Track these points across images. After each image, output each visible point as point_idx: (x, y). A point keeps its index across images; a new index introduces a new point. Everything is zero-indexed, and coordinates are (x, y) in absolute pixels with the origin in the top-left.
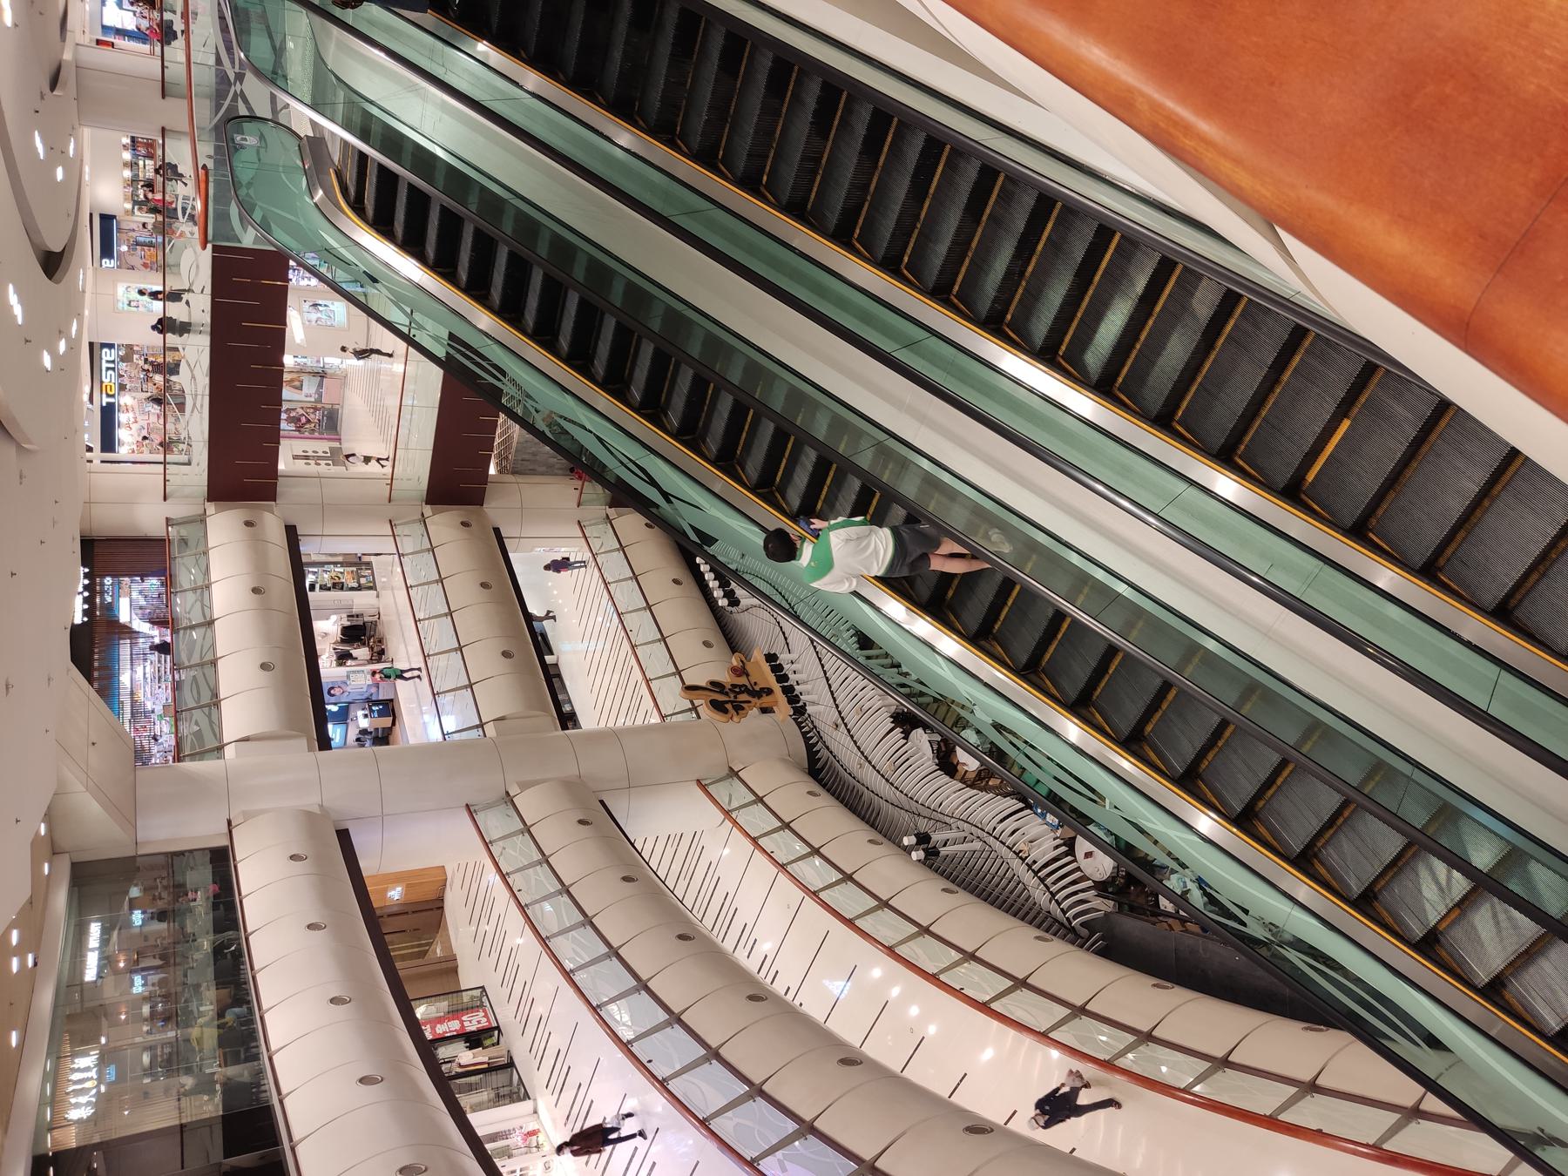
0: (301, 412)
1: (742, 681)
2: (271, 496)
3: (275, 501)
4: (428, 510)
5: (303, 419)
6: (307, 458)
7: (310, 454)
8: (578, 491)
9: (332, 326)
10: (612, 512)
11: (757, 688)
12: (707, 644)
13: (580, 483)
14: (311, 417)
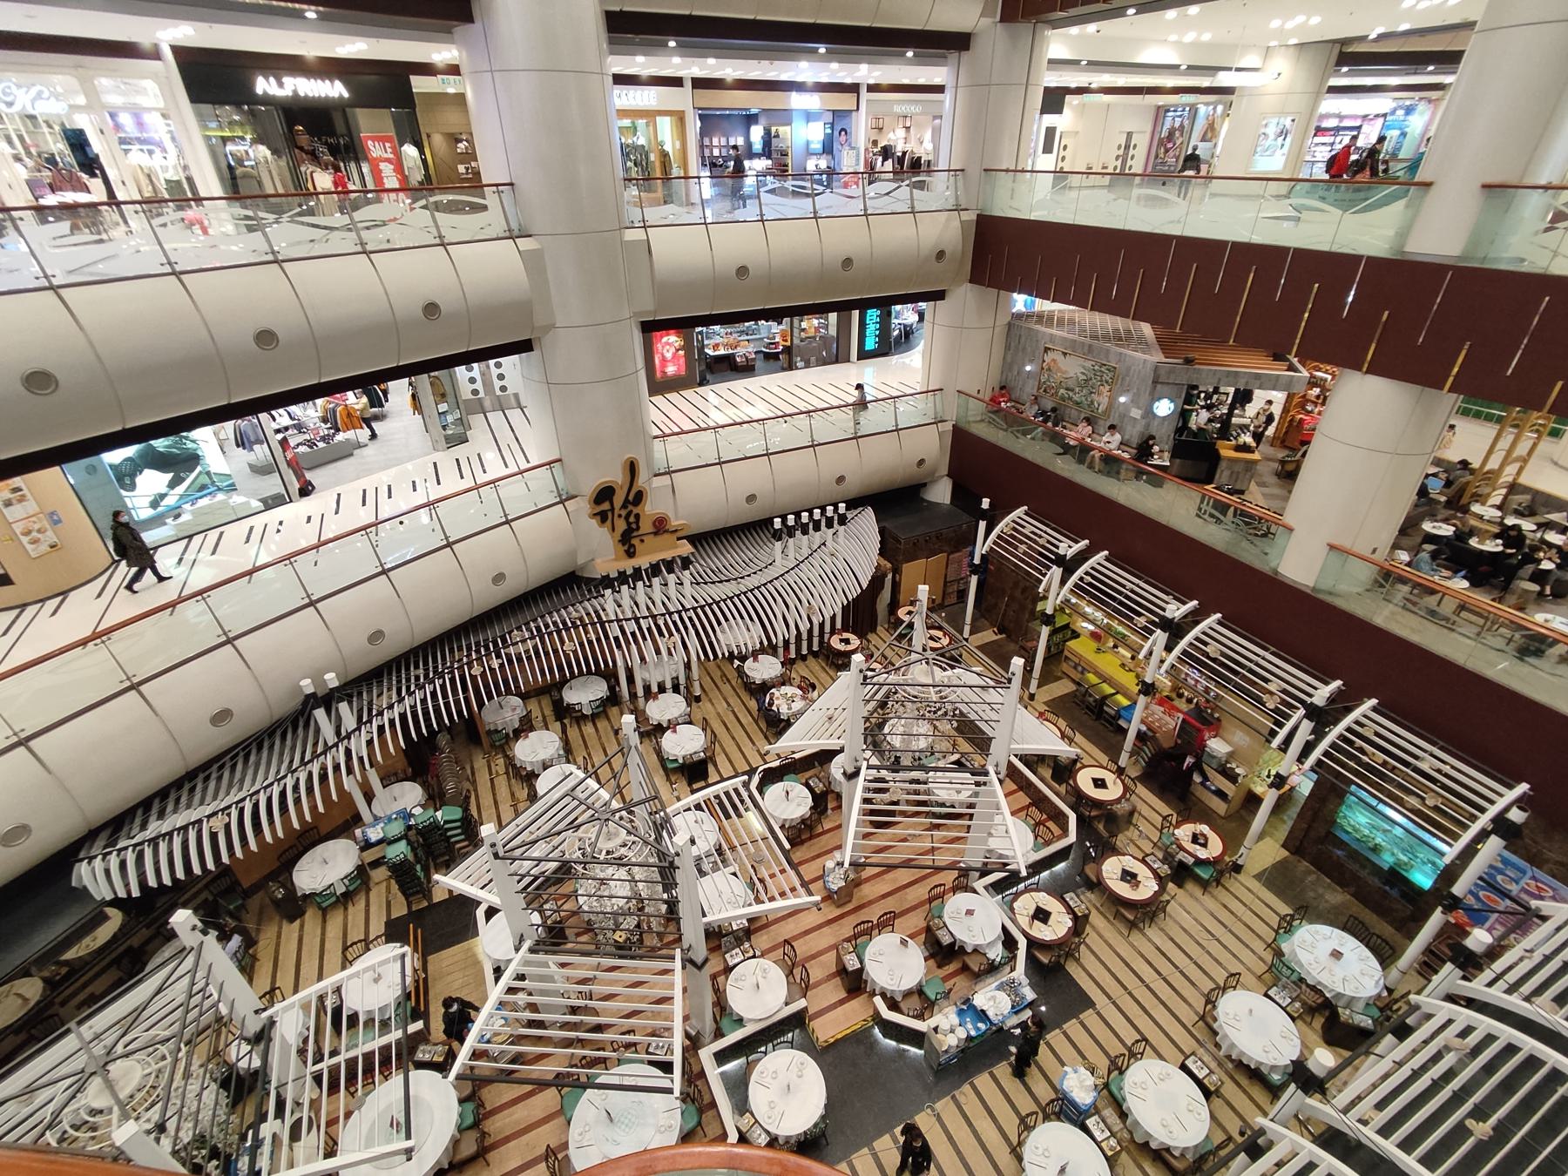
0: (1178, 142)
1: (646, 526)
2: (1006, 17)
3: (1001, 21)
4: (970, 216)
5: (1170, 145)
6: (1127, 147)
7: (1131, 152)
8: (975, 394)
9: (1255, 152)
10: (948, 427)
11: (635, 542)
12: (751, 498)
13: (987, 398)
14: (1171, 153)
